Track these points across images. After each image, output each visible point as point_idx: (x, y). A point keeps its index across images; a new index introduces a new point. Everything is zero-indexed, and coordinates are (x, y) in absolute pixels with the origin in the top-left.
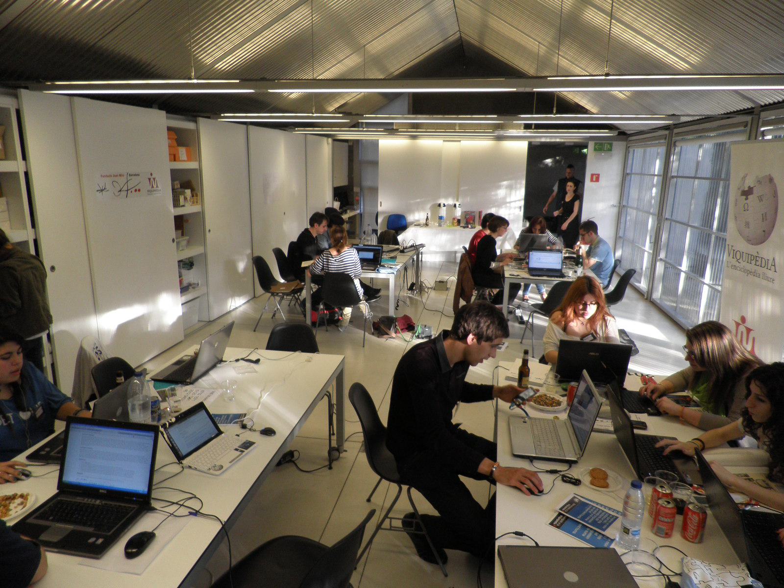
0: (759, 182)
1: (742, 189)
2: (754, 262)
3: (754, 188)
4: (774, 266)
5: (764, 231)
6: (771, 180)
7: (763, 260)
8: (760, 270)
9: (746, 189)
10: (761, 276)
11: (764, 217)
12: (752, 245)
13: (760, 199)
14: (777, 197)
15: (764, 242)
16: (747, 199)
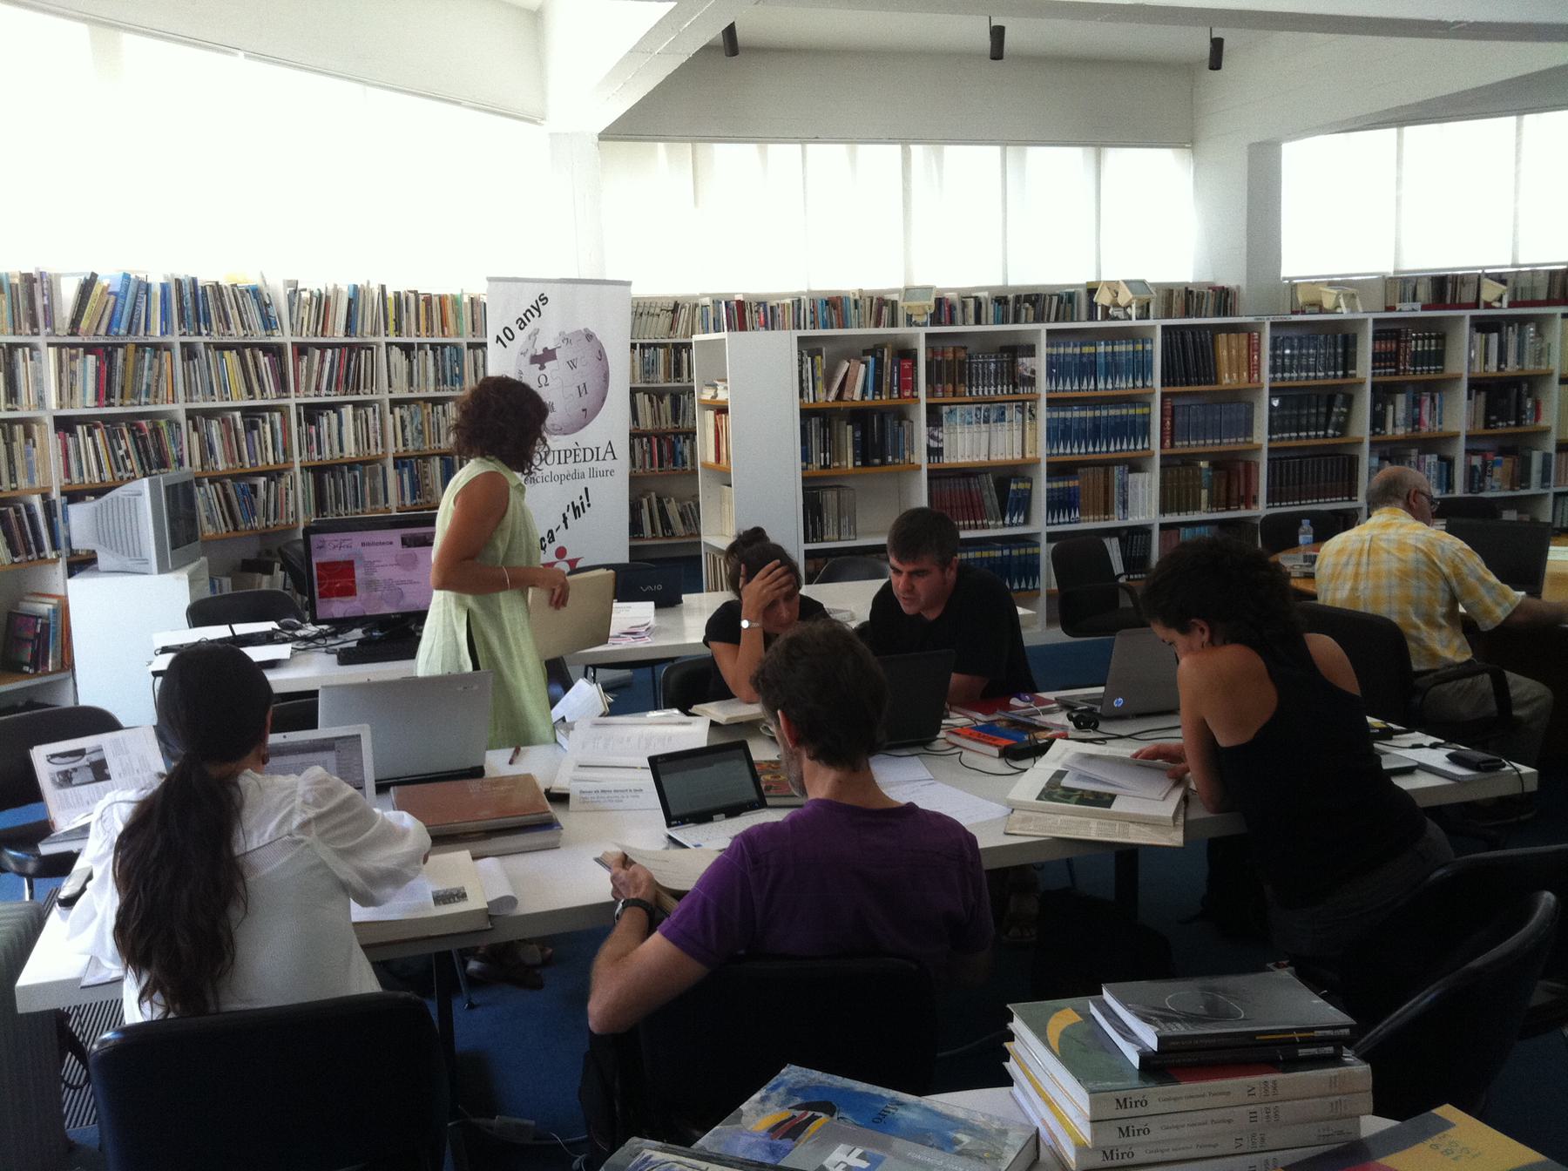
0: (567, 340)
1: (531, 352)
2: (571, 460)
3: (558, 353)
4: (613, 452)
5: (584, 410)
6: (590, 337)
7: (588, 453)
8: (583, 467)
9: (540, 352)
10: (587, 475)
11: (582, 390)
12: (565, 434)
13: (572, 364)
14: (606, 359)
15: (585, 425)
16: (542, 368)
